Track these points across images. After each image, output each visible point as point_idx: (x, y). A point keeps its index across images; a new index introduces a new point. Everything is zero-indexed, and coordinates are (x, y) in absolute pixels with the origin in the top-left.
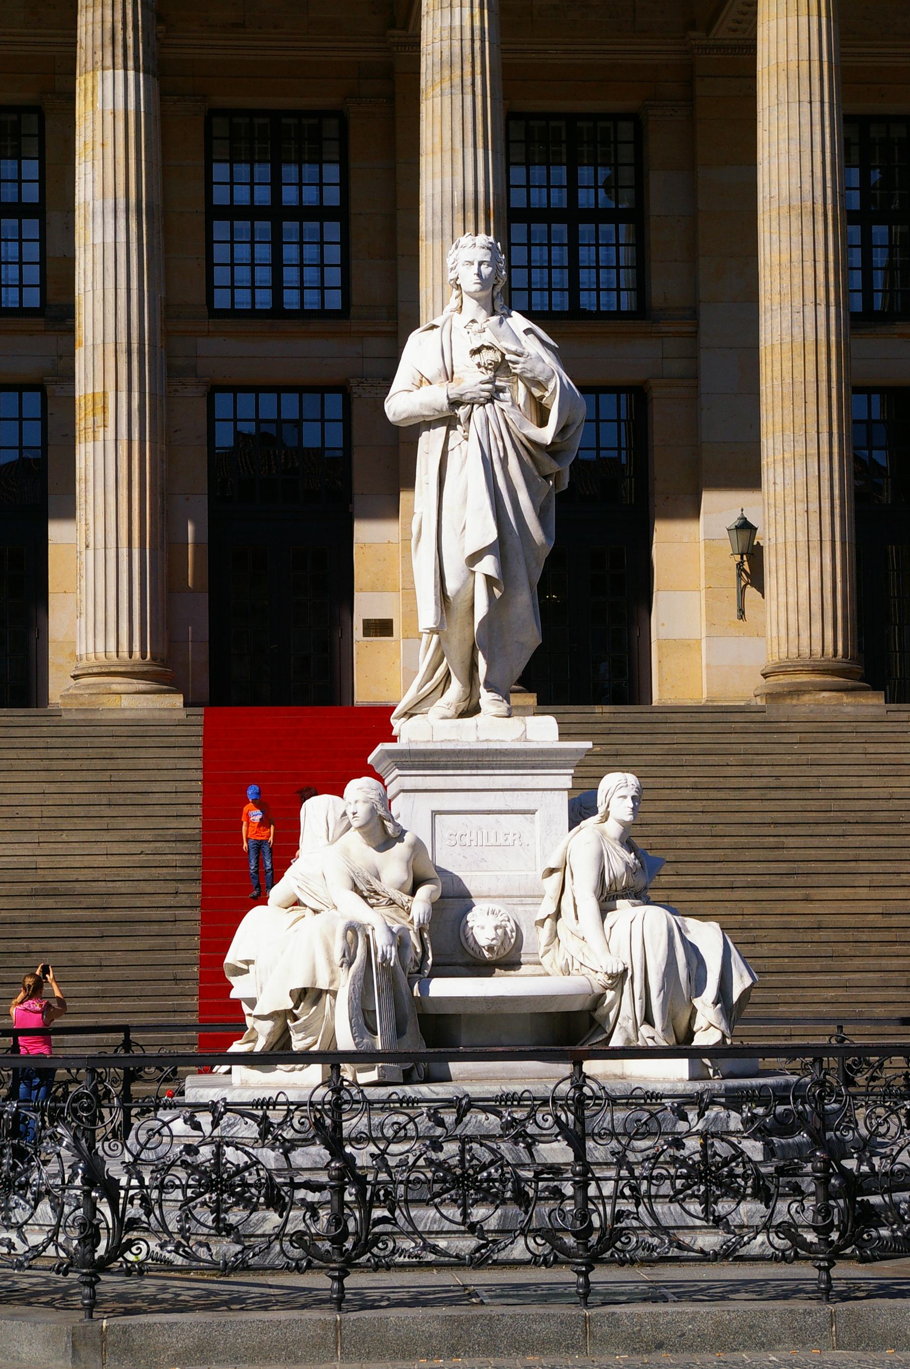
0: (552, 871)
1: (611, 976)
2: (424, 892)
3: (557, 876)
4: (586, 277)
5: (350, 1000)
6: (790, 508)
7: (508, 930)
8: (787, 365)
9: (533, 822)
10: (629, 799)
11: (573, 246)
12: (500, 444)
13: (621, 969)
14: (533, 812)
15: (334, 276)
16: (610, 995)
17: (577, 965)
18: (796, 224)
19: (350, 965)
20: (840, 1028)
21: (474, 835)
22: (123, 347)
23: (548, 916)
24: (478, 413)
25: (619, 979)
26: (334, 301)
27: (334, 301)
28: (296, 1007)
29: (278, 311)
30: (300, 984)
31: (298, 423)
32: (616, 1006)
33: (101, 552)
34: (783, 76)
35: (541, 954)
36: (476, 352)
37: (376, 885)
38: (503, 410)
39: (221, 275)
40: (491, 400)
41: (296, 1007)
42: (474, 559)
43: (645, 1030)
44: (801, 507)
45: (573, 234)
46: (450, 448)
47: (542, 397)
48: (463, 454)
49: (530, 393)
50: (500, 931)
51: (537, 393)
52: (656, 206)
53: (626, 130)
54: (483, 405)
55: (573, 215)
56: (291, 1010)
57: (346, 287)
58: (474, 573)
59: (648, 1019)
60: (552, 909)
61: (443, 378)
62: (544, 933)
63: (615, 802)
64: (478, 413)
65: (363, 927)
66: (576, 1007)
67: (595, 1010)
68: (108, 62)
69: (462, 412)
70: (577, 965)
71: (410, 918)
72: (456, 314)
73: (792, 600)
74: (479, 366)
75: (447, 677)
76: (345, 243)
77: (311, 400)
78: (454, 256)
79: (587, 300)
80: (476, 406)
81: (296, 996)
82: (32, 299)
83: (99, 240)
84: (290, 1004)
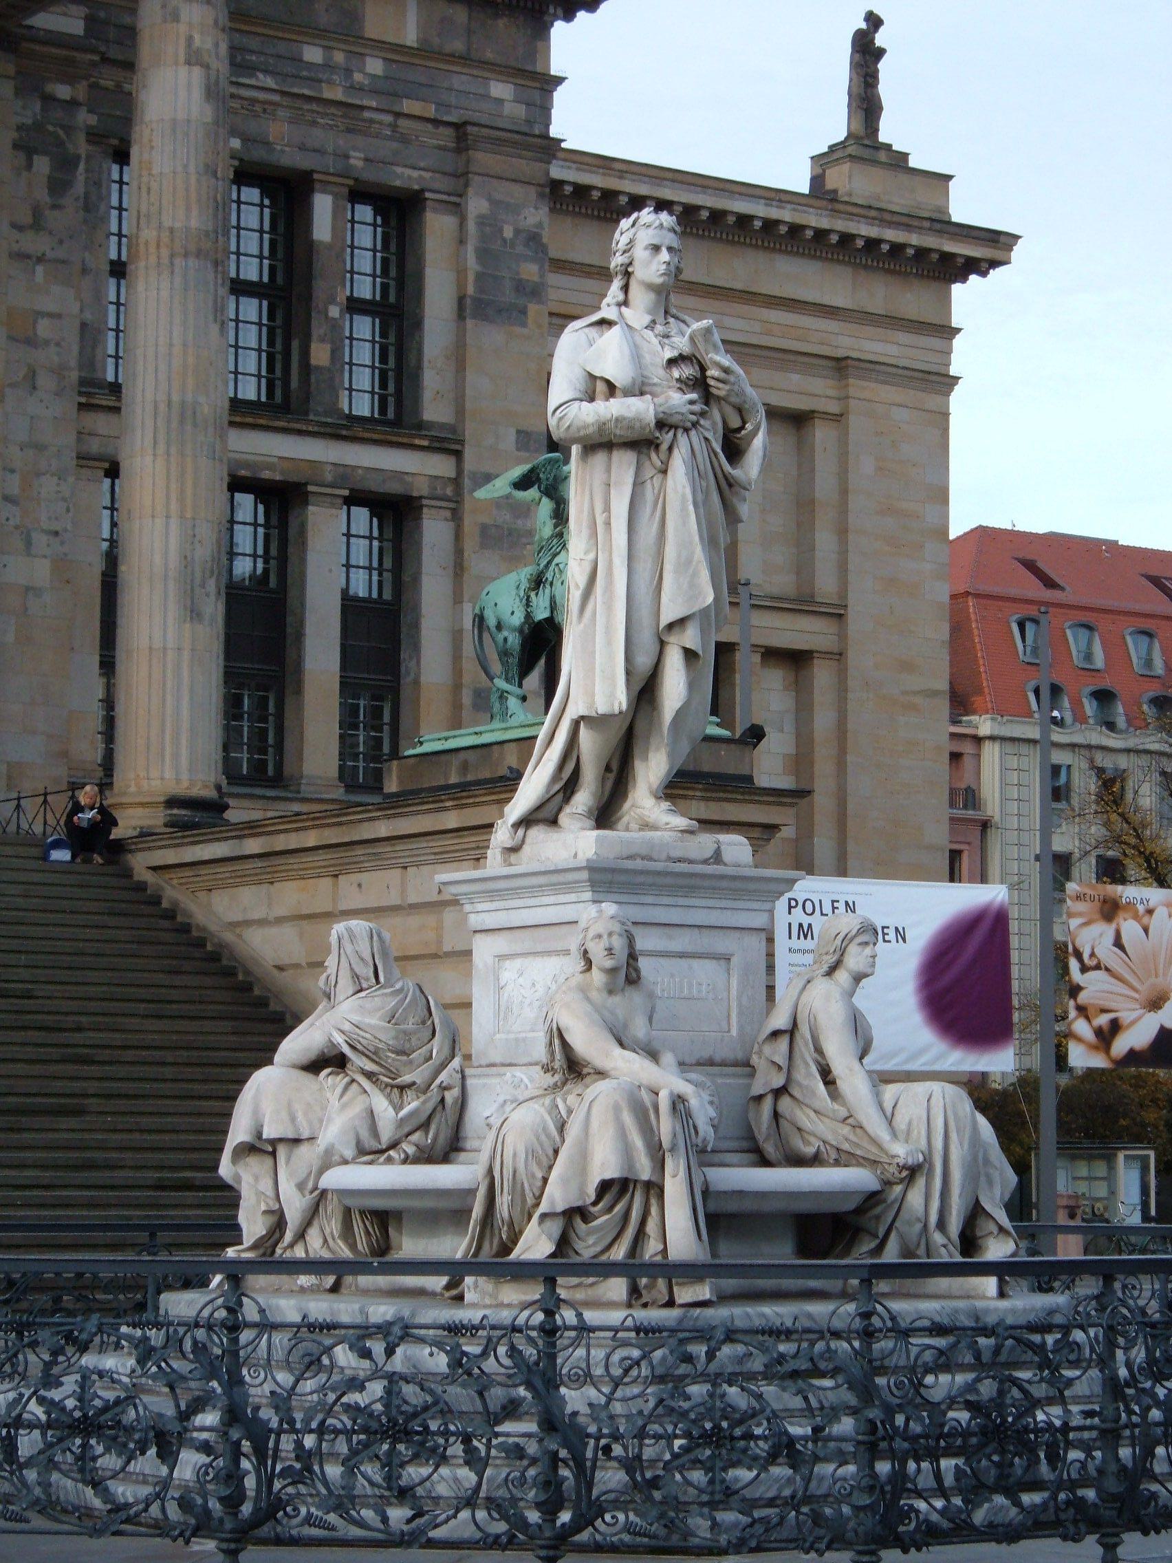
1: (904, 1167)
3: (783, 1043)
20: (153, 1235)
24: (682, 439)
25: (912, 1172)
28: (595, 1204)
36: (672, 362)
42: (678, 624)
51: (735, 422)
54: (686, 430)
59: (942, 1225)
63: (853, 949)
64: (682, 439)
70: (833, 1155)
72: (623, 309)
78: (629, 234)
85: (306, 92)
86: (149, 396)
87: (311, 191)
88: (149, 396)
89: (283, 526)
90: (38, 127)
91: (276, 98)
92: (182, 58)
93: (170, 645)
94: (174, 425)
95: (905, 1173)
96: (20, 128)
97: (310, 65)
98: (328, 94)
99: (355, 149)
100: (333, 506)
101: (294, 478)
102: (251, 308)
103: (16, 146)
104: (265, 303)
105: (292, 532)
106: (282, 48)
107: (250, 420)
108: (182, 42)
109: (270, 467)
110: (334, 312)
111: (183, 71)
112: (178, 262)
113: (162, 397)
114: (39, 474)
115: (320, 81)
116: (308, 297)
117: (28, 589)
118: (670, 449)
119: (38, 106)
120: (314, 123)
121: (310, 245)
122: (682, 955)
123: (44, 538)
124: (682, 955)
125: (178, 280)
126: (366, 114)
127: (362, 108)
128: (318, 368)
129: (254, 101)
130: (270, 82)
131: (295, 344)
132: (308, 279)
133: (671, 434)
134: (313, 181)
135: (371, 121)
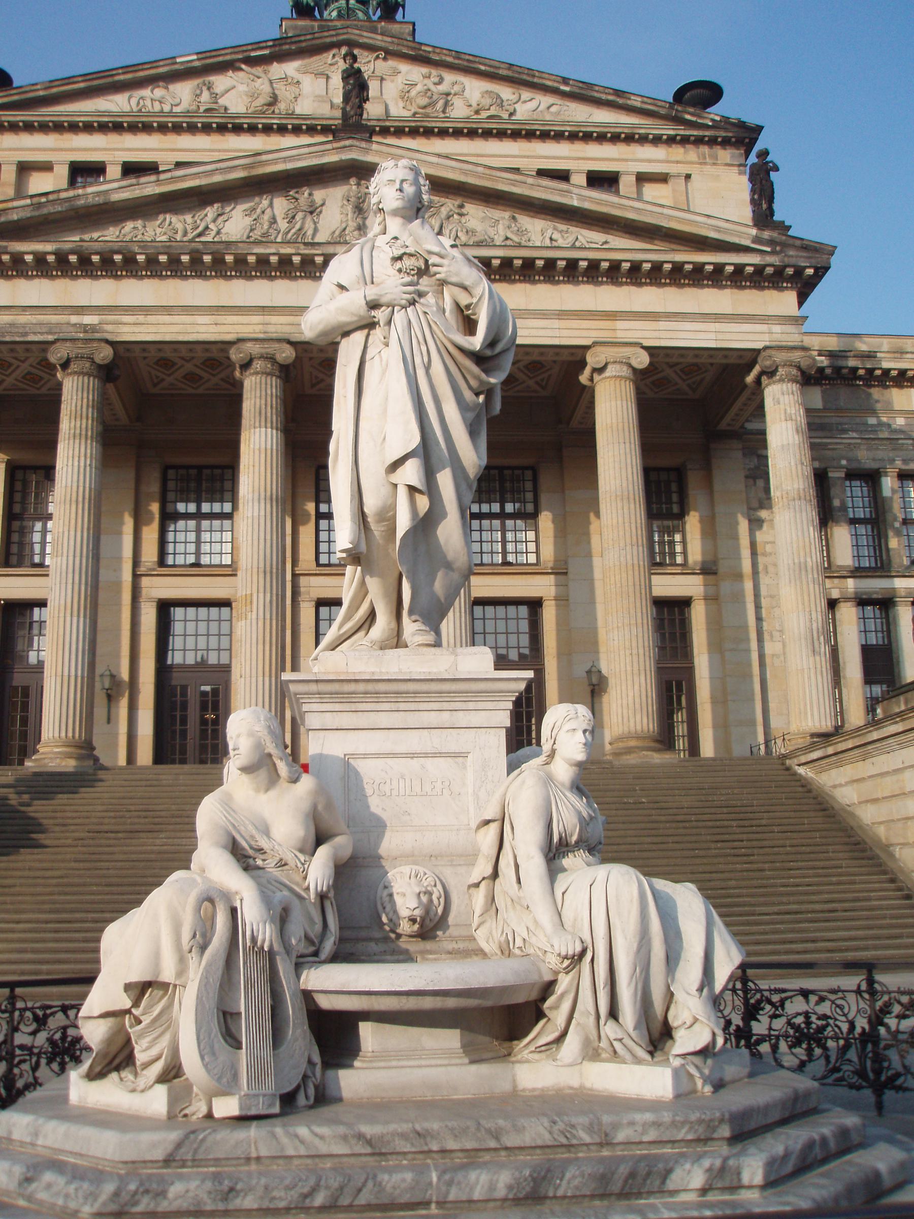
0: (487, 822)
2: (323, 852)
5: (199, 999)
6: (622, 653)
7: (434, 897)
8: (618, 577)
9: (465, 767)
10: (580, 733)
12: (424, 348)
13: (578, 948)
14: (463, 755)
16: (564, 982)
17: (519, 942)
18: (620, 505)
19: (203, 948)
21: (395, 782)
22: (261, 570)
23: (484, 879)
30: (137, 976)
32: (571, 996)
33: (248, 679)
34: (610, 430)
35: (474, 926)
37: (263, 843)
38: (425, 313)
40: (413, 303)
41: (136, 1004)
43: (610, 1029)
44: (628, 652)
45: (503, 526)
46: (368, 357)
47: (468, 307)
48: (384, 362)
49: (457, 305)
50: (424, 899)
51: (464, 300)
53: (529, 474)
54: (404, 307)
55: (502, 516)
56: (128, 1011)
58: (396, 485)
60: (489, 871)
61: (361, 281)
62: (479, 897)
65: (227, 896)
66: (520, 999)
67: (544, 999)
68: (257, 424)
71: (306, 884)
73: (625, 702)
74: (400, 271)
75: (372, 616)
80: (396, 308)
81: (136, 992)
82: (227, 560)
83: (250, 515)
84: (127, 1003)
85: (872, 436)
86: (786, 562)
87: (880, 477)
88: (786, 562)
89: (887, 617)
90: (757, 468)
91: (859, 441)
92: (783, 418)
93: (805, 667)
94: (797, 572)
95: (566, 962)
96: (749, 470)
97: (872, 425)
98: (881, 436)
99: (898, 456)
100: (906, 606)
101: (887, 596)
102: (862, 529)
103: (747, 477)
104: (869, 527)
105: (891, 620)
106: (858, 420)
107: (864, 574)
108: (783, 412)
109: (876, 593)
110: (897, 525)
111: (784, 424)
112: (791, 503)
113: (790, 562)
114: (773, 608)
115: (876, 431)
116: (885, 521)
117: (773, 655)
118: (389, 323)
119: (756, 460)
120: (877, 449)
121: (884, 499)
122: (413, 756)
123: (778, 634)
124: (413, 756)
125: (792, 510)
126: (900, 442)
127: (898, 439)
128: (893, 549)
129: (850, 444)
130: (855, 435)
131: (883, 540)
132: (884, 512)
133: (390, 308)
134: (880, 473)
135: (903, 444)
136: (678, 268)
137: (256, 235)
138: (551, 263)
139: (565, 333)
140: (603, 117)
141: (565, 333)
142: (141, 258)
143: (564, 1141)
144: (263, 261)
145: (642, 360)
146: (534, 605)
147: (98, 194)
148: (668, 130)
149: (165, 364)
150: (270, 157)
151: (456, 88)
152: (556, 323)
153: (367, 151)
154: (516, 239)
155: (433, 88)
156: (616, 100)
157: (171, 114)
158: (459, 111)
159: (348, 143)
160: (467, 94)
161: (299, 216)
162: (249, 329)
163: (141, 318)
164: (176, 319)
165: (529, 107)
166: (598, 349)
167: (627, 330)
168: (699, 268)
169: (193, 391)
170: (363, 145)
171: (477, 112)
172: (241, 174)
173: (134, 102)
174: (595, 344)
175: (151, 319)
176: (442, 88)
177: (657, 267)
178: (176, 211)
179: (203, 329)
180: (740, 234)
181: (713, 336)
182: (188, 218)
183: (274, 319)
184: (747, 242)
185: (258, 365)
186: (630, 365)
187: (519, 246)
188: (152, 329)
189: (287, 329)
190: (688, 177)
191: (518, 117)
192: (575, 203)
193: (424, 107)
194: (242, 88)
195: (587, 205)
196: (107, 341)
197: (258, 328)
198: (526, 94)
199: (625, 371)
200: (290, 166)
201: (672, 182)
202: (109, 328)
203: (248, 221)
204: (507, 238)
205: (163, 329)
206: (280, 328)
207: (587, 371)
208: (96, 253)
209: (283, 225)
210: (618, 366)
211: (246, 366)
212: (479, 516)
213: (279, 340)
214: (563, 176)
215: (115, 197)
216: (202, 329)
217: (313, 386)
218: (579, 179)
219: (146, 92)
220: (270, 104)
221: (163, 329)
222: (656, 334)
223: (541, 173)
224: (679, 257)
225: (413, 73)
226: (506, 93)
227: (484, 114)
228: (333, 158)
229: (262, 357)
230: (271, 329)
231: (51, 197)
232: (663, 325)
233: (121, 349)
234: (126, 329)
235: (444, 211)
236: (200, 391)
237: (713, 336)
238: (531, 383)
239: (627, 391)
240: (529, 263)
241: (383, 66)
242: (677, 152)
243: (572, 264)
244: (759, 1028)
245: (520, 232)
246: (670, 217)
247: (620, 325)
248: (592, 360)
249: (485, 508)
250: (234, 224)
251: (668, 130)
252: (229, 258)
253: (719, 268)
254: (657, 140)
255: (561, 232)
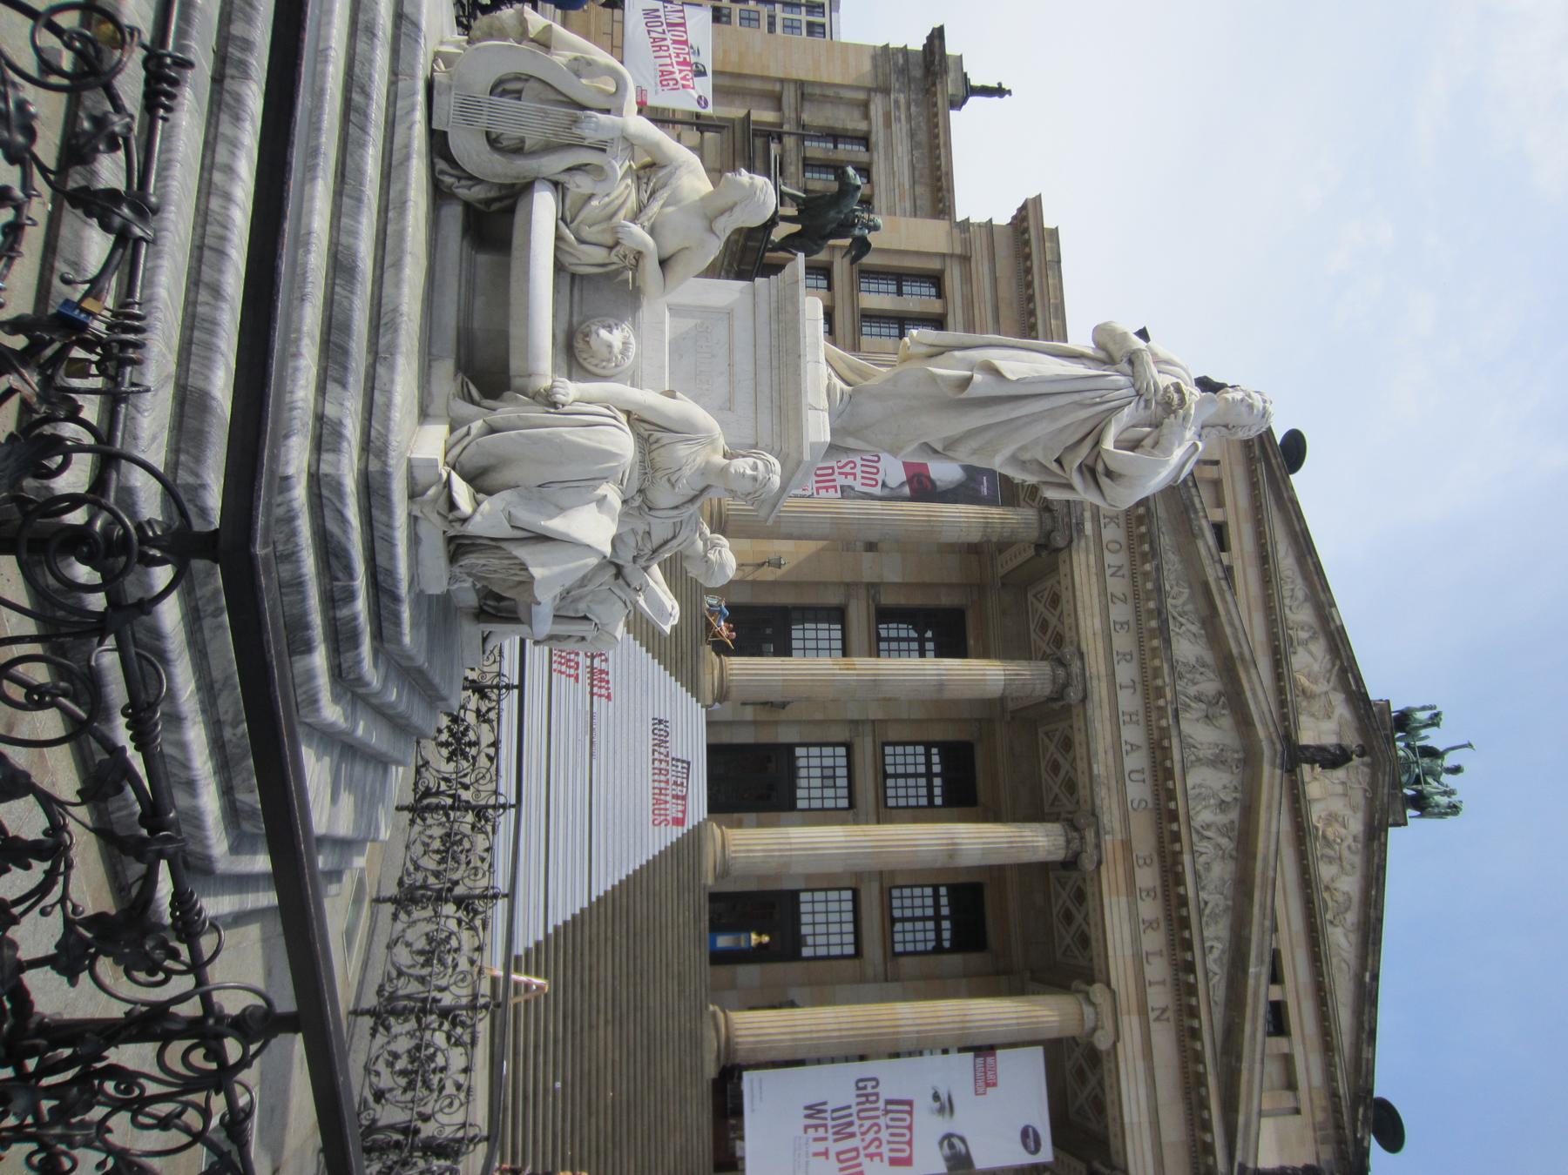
4: (909, 926)
11: (924, 919)
15: (902, 802)
24: (1122, 380)
26: (891, 802)
27: (891, 802)
29: (886, 776)
31: (835, 787)
39: (899, 750)
40: (1139, 394)
51: (1148, 442)
52: (945, 958)
57: (897, 807)
69: (1125, 367)
76: (918, 807)
77: (844, 792)
79: (898, 926)
136: (1200, 1080)
137: (1180, 668)
138: (1188, 945)
139: (1120, 961)
140: (1344, 1017)
141: (1120, 961)
142: (1148, 567)
143: (383, 322)
144: (1157, 672)
145: (1102, 1042)
146: (858, 954)
147: (1201, 529)
148: (1343, 1089)
149: (1055, 600)
150: (1254, 677)
151: (1347, 867)
152: (1128, 952)
153: (1273, 764)
154: (1207, 911)
155: (1345, 844)
156: (1366, 1032)
157: (1282, 606)
158: (1326, 871)
159: (1279, 747)
160: (1345, 878)
161: (1204, 706)
162: (1093, 663)
163: (1093, 570)
164: (1096, 601)
165: (1341, 940)
166: (1108, 996)
167: (1131, 1025)
168: (1204, 1104)
169: (1032, 627)
170: (1278, 761)
171: (1327, 888)
172: (1235, 651)
173: (1289, 573)
174: (1113, 992)
175: (1094, 579)
176: (1346, 853)
177: (1198, 1058)
178: (1192, 597)
179: (1090, 624)
180: (1246, 1150)
181: (1135, 1120)
182: (1189, 607)
183: (1104, 685)
184: (1239, 1157)
185: (1061, 672)
186: (1094, 1030)
187: (1200, 913)
188: (1085, 580)
189: (1096, 697)
190: (1297, 1111)
191: (1330, 929)
192: (1252, 970)
193: (1324, 837)
194: (1316, 667)
195: (1251, 982)
196: (1071, 541)
197: (1094, 670)
198: (1353, 937)
199: (1089, 1024)
200: (1248, 694)
201: (1289, 1094)
202: (1083, 544)
203: (1193, 661)
204: (1206, 903)
205: (1086, 590)
206: (1096, 690)
207: (1083, 987)
208: (1149, 530)
209: (1192, 691)
210: (1092, 1016)
211: (1061, 662)
212: (936, 896)
213: (1085, 690)
214: (1276, 977)
215: (1200, 544)
216: (1089, 623)
217: (1046, 734)
218: (1275, 993)
219: (1299, 581)
220: (1304, 692)
221: (1086, 590)
222: (1130, 1054)
223: (1276, 956)
224: (1212, 1081)
225: (1356, 825)
226: (1351, 917)
227: (1326, 895)
228: (1261, 734)
229: (1068, 675)
230: (1095, 683)
231: (1193, 490)
232: (1140, 1064)
233: (1063, 556)
234: (1083, 557)
235: (1224, 841)
236: (1033, 636)
237: (1135, 1120)
238: (1068, 940)
239: (1071, 1029)
240: (1185, 923)
241: (1358, 797)
242: (1321, 1101)
243: (1190, 967)
244: (449, 909)
245: (1214, 917)
246: (1251, 1070)
247: (1135, 1020)
248: (1097, 990)
249: (944, 901)
250: (1188, 647)
251: (1343, 1089)
252: (1155, 643)
253: (1206, 1126)
254: (1330, 1077)
255: (1220, 958)
